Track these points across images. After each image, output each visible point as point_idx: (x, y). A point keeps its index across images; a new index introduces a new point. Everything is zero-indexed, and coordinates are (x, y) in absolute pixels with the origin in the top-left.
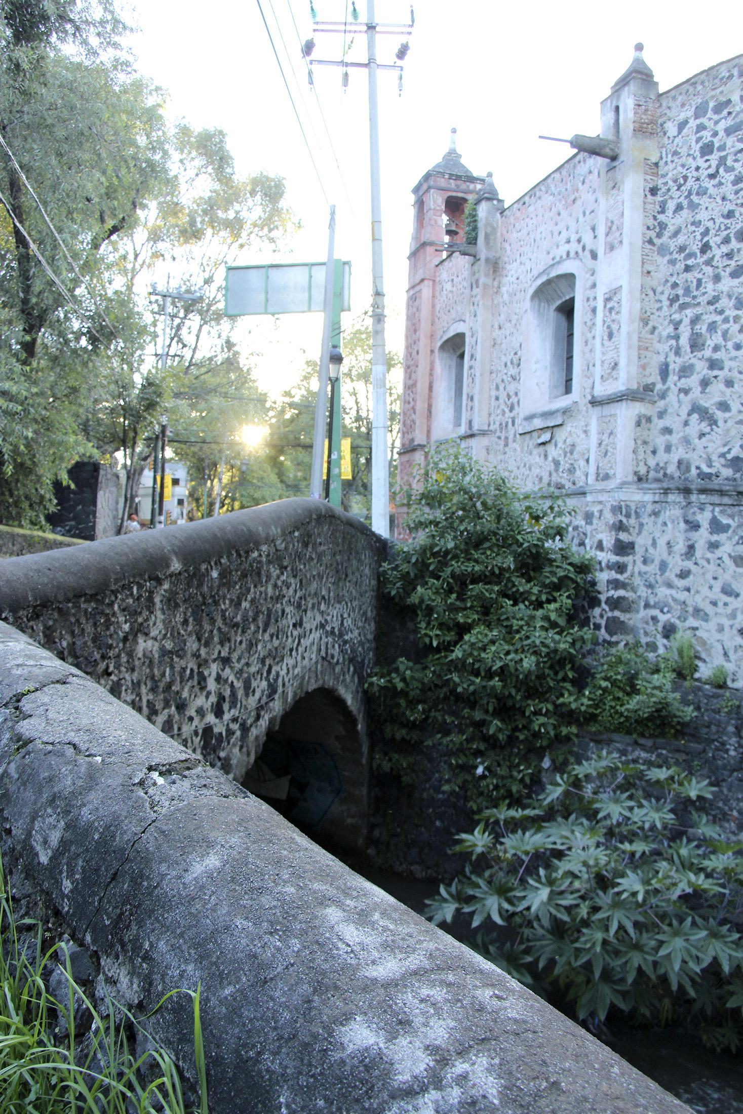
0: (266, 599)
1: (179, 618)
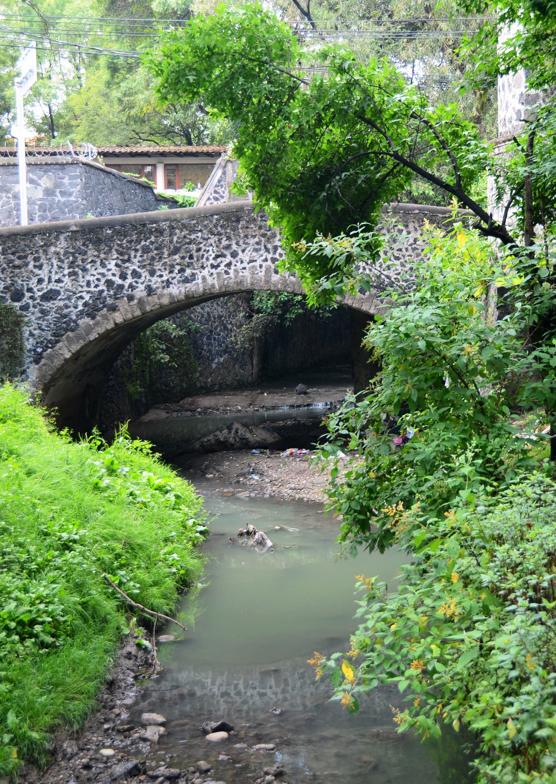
1: (79, 244)
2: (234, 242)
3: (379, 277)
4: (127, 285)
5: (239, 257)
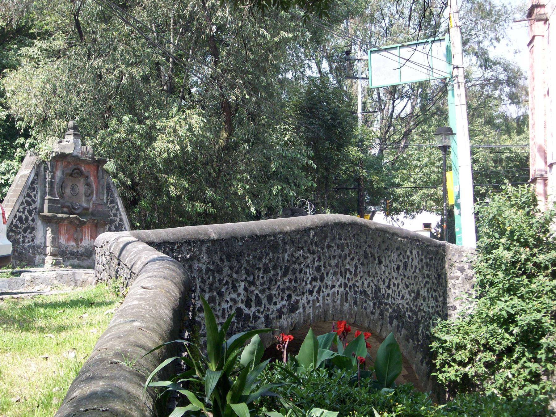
0: (283, 261)
1: (217, 258)
2: (322, 263)
3: (399, 306)
4: (251, 316)
5: (325, 281)
